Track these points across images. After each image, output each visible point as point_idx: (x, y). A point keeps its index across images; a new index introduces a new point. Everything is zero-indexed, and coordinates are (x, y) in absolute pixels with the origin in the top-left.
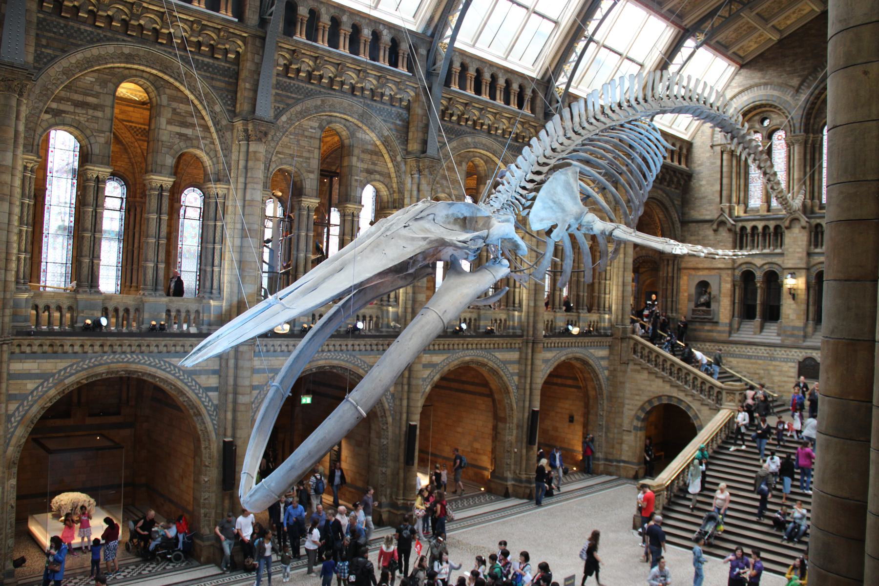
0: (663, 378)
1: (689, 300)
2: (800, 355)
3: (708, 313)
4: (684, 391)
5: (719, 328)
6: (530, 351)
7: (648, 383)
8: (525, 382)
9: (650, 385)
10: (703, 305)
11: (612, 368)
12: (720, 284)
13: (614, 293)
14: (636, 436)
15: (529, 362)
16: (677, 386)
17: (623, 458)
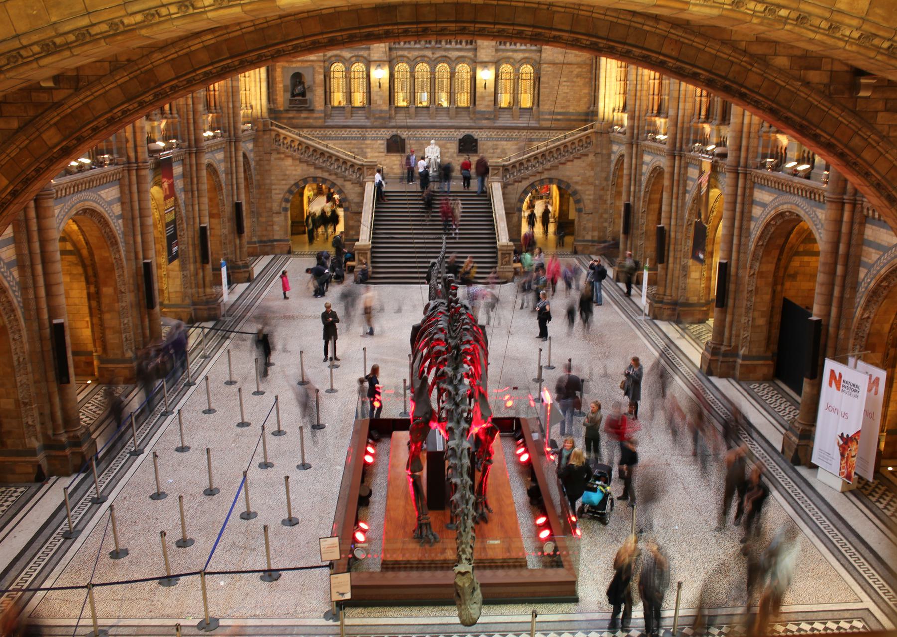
0: (307, 163)
1: (285, 91)
2: (387, 133)
3: (305, 102)
4: (328, 171)
5: (315, 115)
6: (233, 149)
7: (293, 168)
8: (232, 179)
9: (295, 170)
10: (298, 95)
11: (257, 159)
12: (314, 75)
13: (253, 89)
14: (286, 217)
15: (234, 160)
16: (321, 168)
17: (276, 237)
